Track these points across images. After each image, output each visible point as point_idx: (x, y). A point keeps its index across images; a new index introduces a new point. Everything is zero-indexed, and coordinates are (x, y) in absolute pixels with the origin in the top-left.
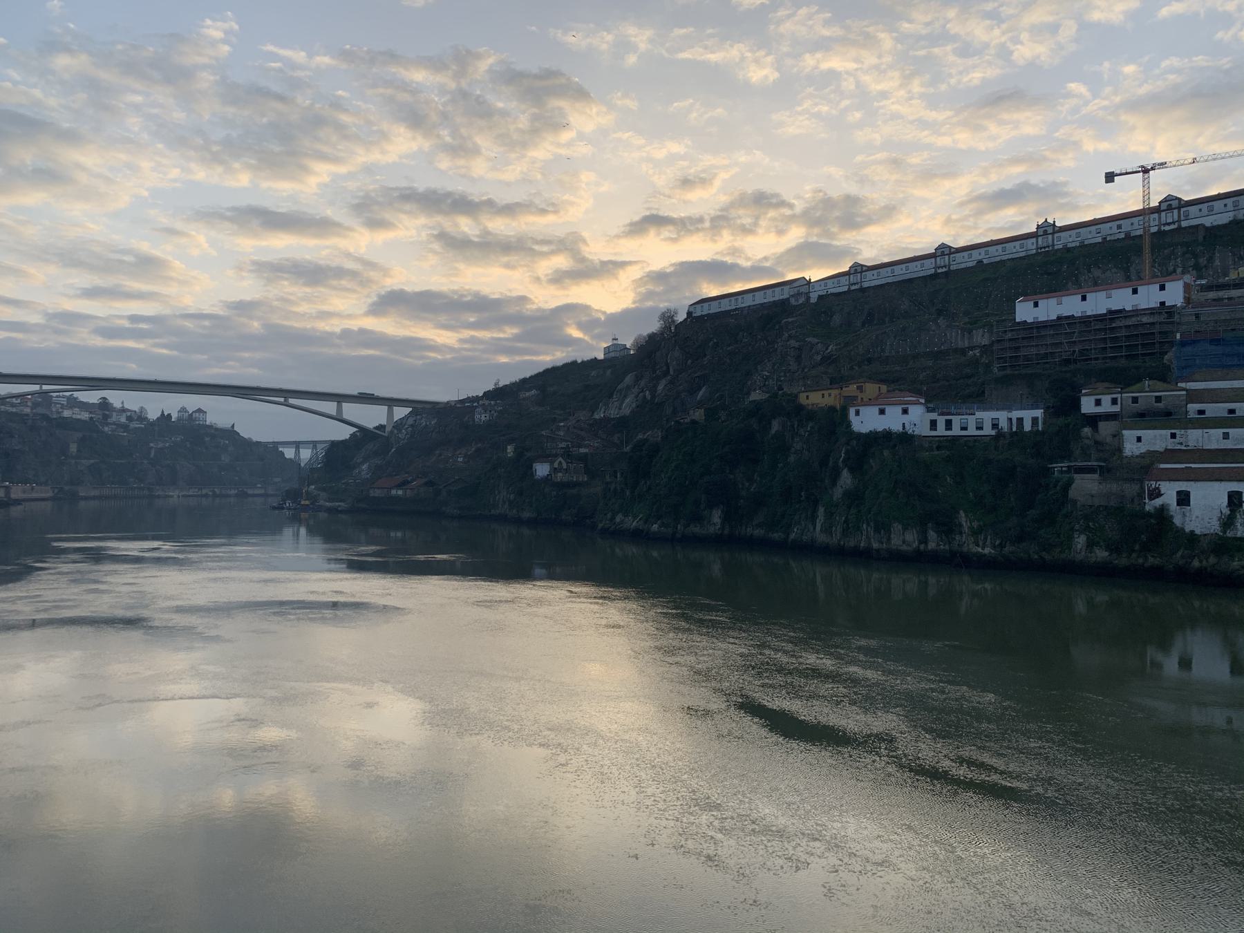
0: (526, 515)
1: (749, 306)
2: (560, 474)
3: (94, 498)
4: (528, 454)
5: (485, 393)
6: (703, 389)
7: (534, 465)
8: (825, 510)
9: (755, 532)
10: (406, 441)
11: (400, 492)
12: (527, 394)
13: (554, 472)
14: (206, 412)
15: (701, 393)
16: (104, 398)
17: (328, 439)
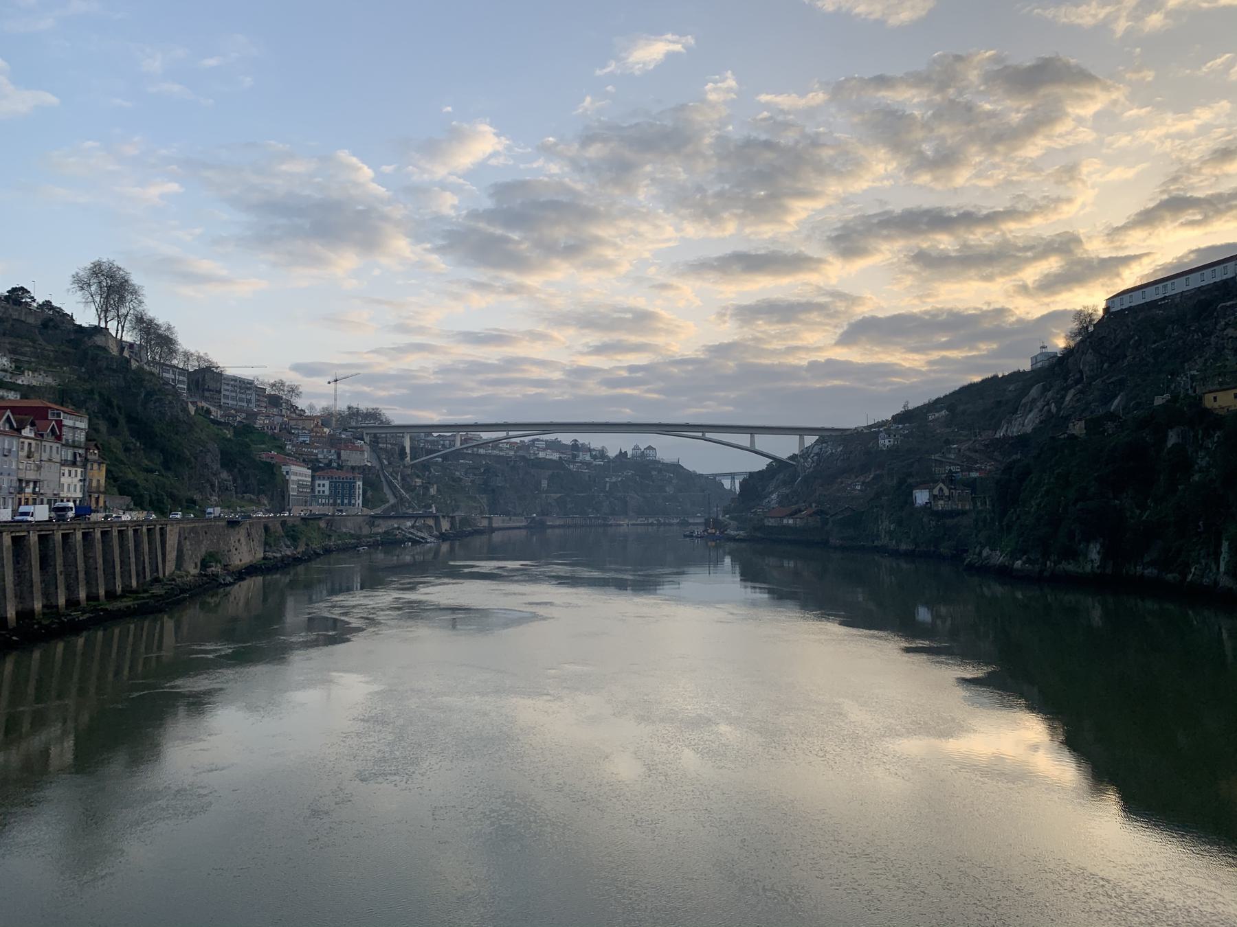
0: (903, 547)
1: (1182, 293)
2: (941, 502)
3: (559, 526)
4: (910, 480)
5: (893, 417)
6: (1119, 398)
7: (914, 492)
8: (1229, 545)
9: (1146, 572)
10: (811, 469)
11: (791, 521)
12: (937, 415)
13: (934, 500)
14: (655, 449)
15: (1116, 402)
16: (576, 440)
17: (749, 470)
